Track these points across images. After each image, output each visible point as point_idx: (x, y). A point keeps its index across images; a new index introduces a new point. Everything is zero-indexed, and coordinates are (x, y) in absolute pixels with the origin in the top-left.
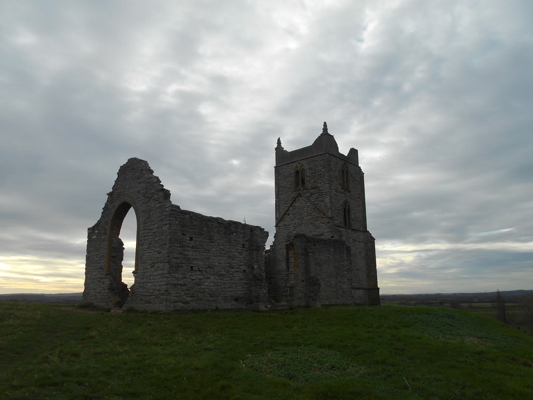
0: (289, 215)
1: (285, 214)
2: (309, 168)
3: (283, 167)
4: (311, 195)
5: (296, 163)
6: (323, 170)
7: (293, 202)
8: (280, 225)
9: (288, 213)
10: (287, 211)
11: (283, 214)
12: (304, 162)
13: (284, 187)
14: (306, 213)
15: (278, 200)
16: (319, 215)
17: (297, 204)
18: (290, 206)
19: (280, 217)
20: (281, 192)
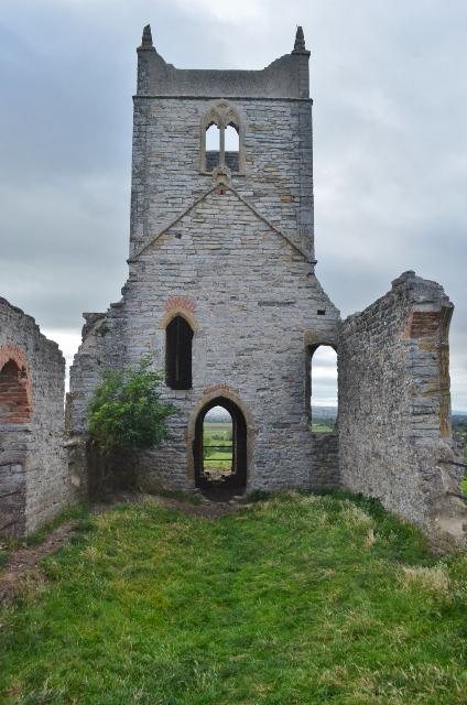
0: (179, 236)
1: (166, 231)
2: (250, 126)
3: (164, 102)
4: (256, 195)
5: (212, 103)
6: (296, 139)
7: (195, 204)
8: (143, 258)
9: (178, 229)
10: (173, 225)
11: (157, 231)
12: (239, 107)
13: (164, 159)
14: (235, 240)
15: (141, 188)
16: (282, 252)
17: (207, 210)
18: (186, 214)
19: (148, 240)
20: (152, 170)
